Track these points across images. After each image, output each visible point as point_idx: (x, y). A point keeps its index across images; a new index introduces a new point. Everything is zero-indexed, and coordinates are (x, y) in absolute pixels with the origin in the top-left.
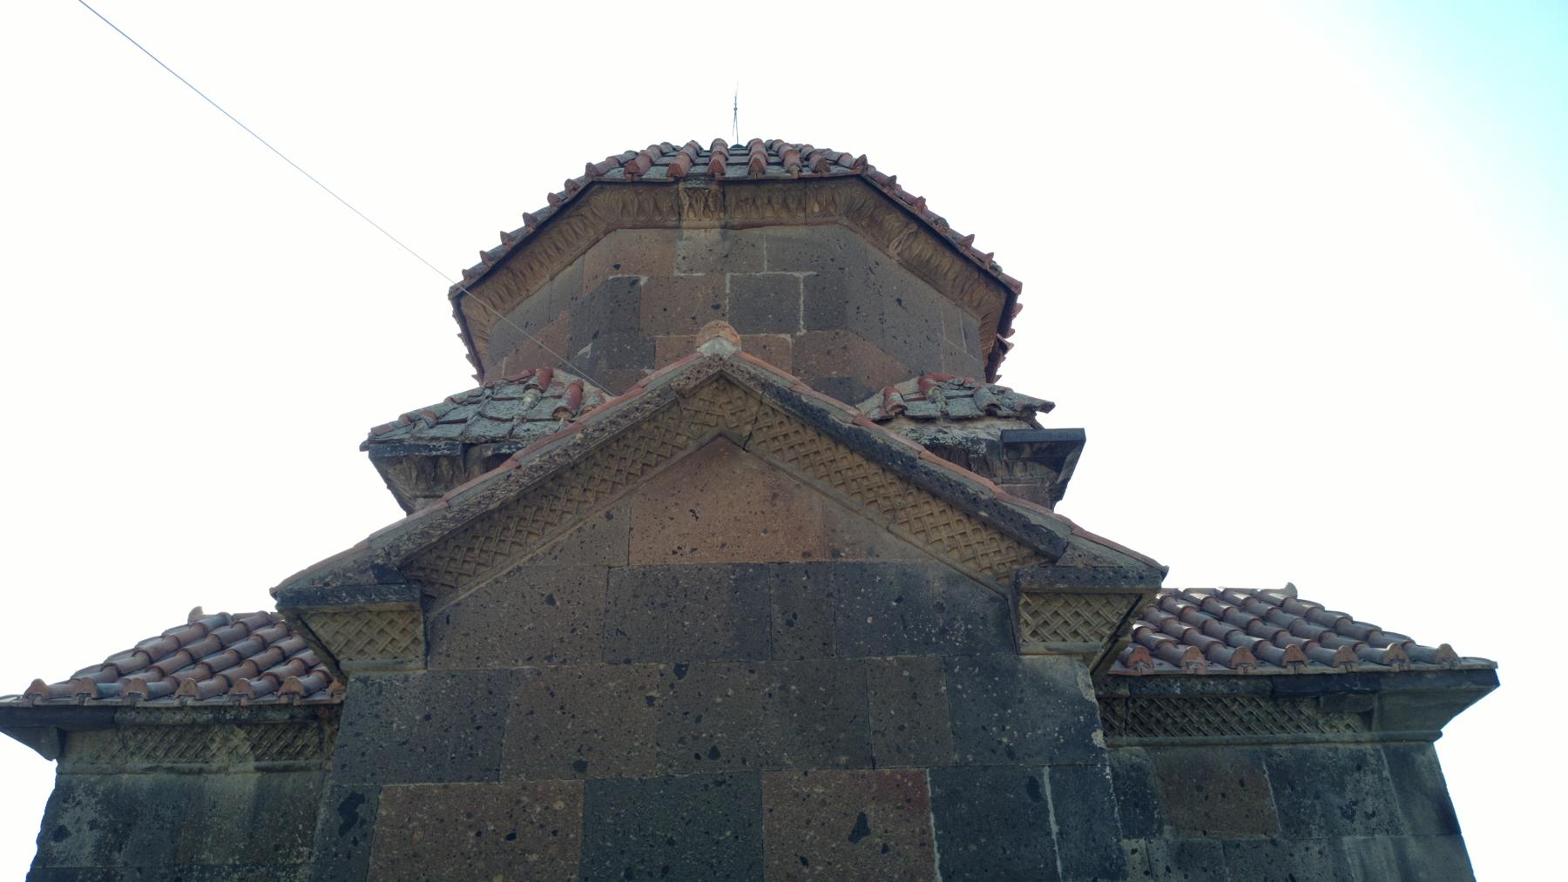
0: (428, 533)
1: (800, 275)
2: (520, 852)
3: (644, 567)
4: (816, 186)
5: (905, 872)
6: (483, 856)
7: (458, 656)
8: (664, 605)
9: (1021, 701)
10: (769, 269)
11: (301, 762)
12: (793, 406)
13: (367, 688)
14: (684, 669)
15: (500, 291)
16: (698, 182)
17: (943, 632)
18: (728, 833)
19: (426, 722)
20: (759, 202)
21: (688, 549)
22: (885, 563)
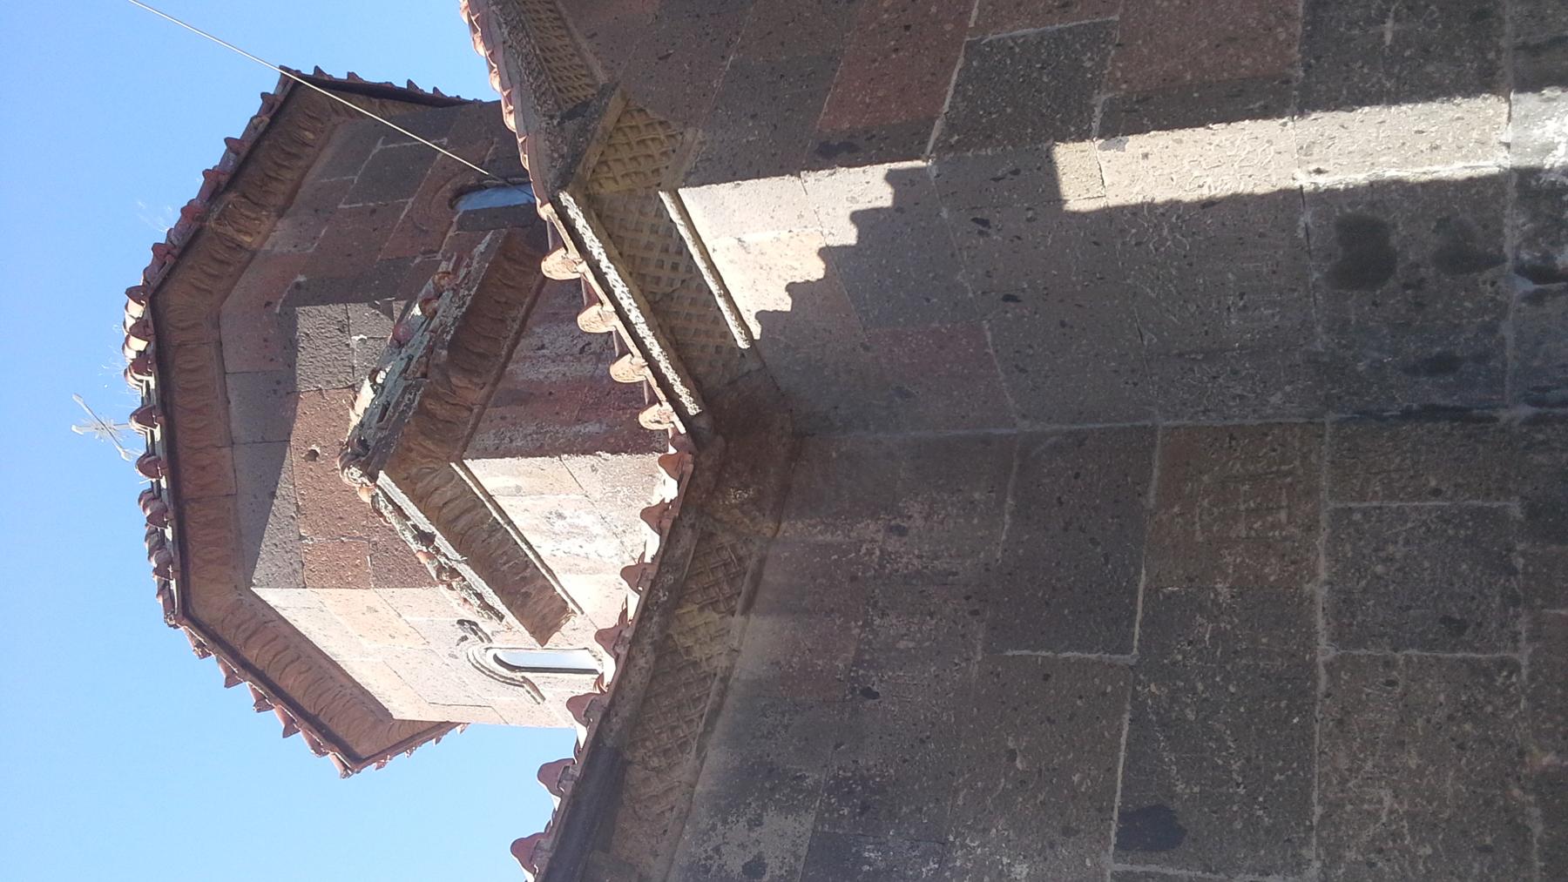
1: (379, 146)
11: (751, 564)
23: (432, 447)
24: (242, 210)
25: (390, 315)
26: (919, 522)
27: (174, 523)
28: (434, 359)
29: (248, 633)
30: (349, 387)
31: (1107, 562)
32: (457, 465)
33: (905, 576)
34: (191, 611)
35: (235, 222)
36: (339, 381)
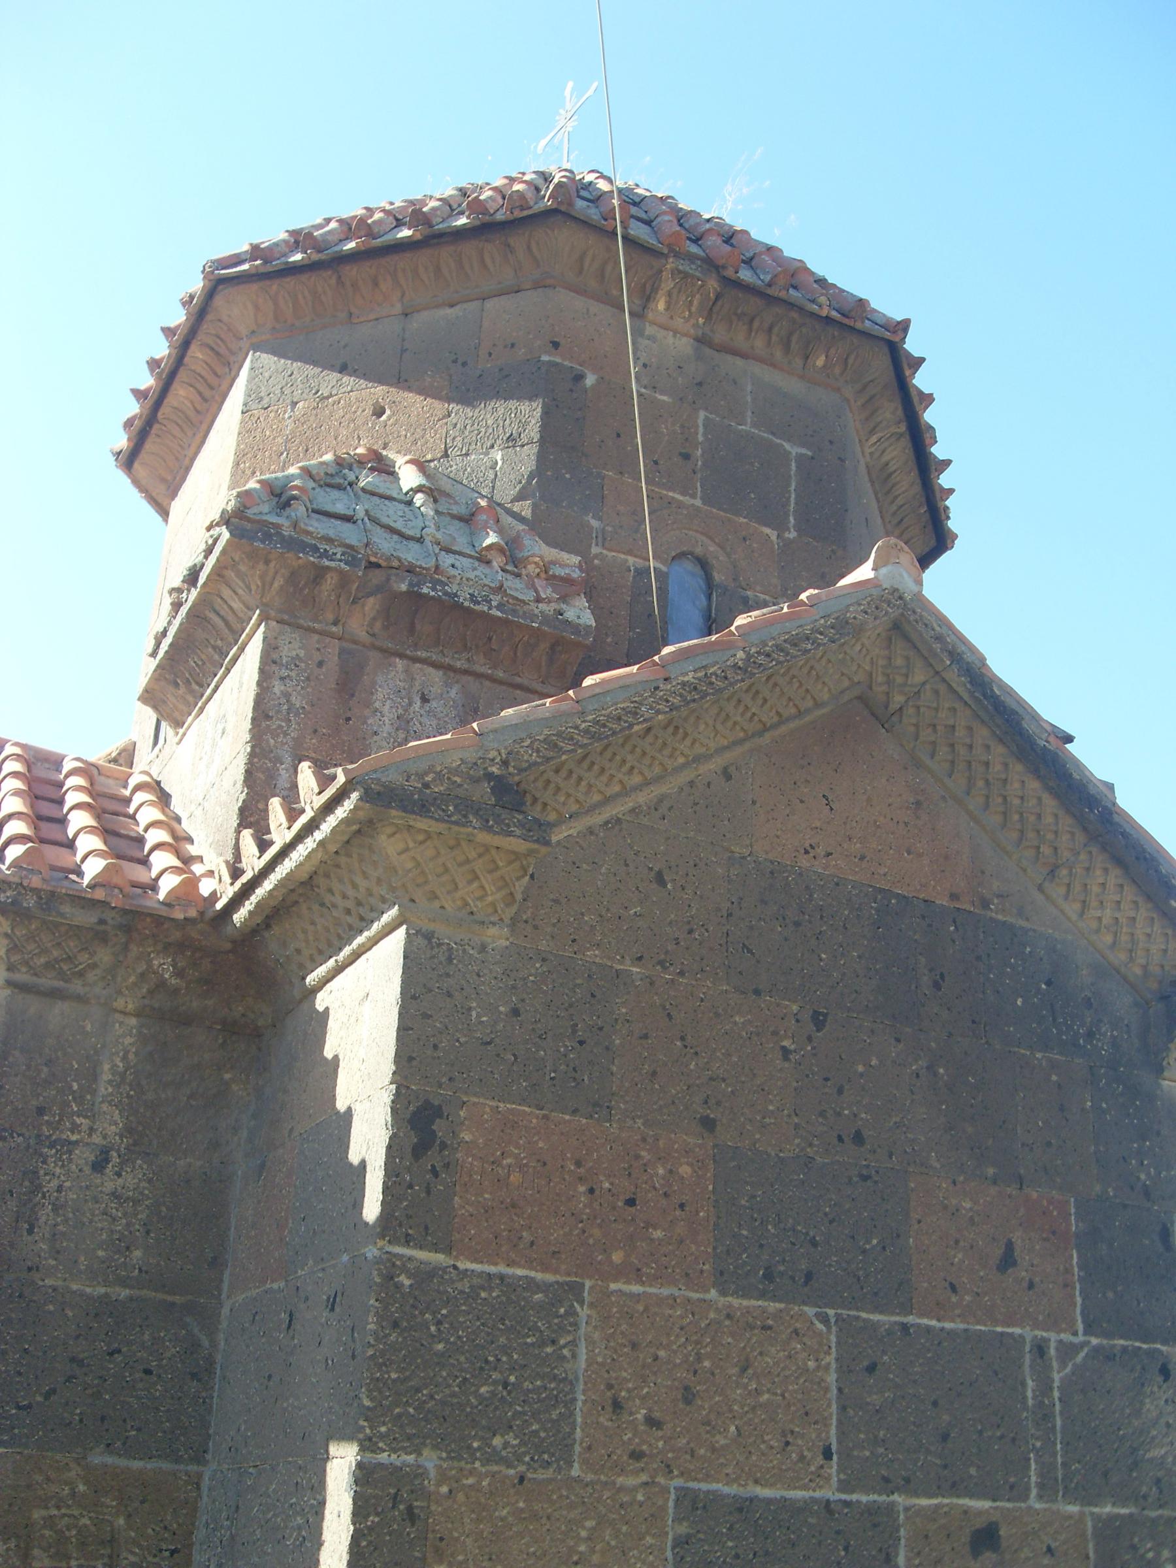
0: (556, 745)
1: (794, 450)
2: (642, 1225)
3: (772, 862)
4: (836, 333)
5: (1049, 1315)
6: (599, 1221)
7: (549, 930)
8: (797, 924)
9: (1158, 1133)
10: (754, 425)
11: (77, 987)
12: (984, 695)
13: (432, 948)
14: (821, 1018)
15: (300, 297)
16: (693, 267)
17: (1090, 1035)
18: (875, 1242)
19: (515, 1019)
20: (756, 324)
21: (820, 851)
22: (1034, 931)
23: (276, 585)
24: (698, 296)
25: (519, 498)
26: (109, 1186)
27: (306, 262)
28: (397, 575)
29: (216, 347)
30: (446, 450)
31: (19, 1408)
32: (259, 615)
33: (36, 1173)
34: (221, 287)
35: (680, 291)
36: (454, 438)
